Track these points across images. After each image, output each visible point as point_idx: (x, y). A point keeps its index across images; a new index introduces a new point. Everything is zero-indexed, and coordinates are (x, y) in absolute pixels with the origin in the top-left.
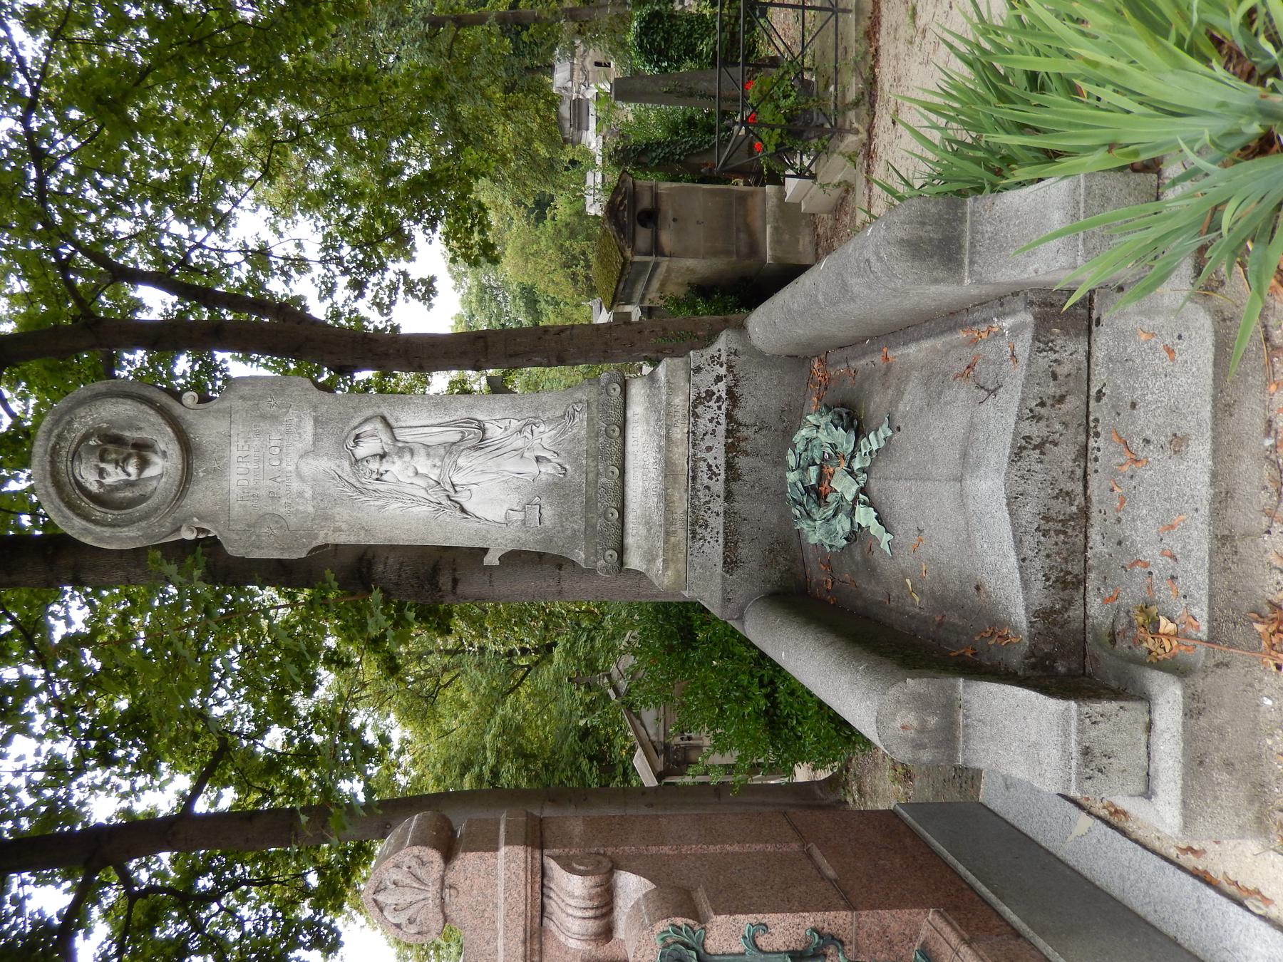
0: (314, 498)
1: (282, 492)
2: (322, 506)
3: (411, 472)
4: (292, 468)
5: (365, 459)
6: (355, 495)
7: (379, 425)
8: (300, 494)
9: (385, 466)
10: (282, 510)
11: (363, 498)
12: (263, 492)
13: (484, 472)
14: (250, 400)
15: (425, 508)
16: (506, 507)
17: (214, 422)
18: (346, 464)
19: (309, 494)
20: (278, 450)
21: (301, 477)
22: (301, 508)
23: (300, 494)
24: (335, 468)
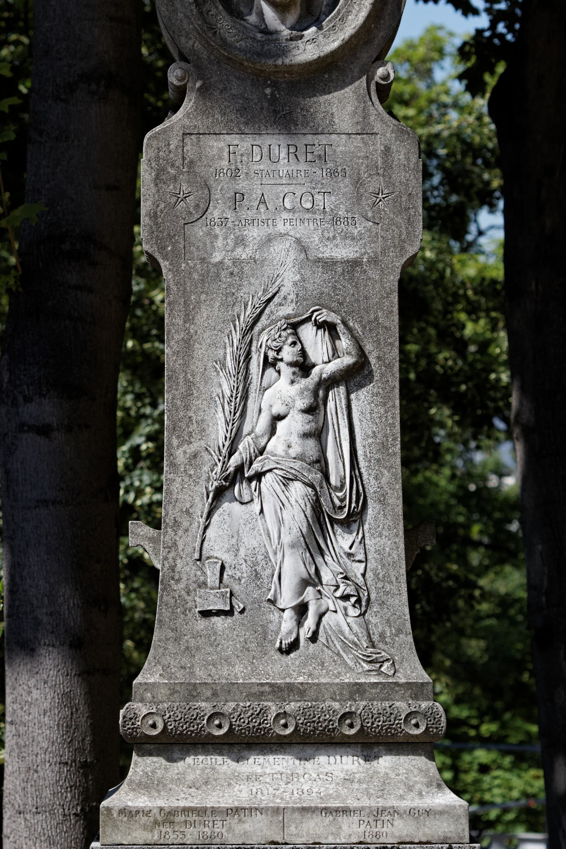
0: (236, 262)
1: (245, 214)
2: (223, 274)
3: (278, 409)
4: (281, 228)
5: (297, 341)
6: (241, 324)
7: (348, 360)
8: (241, 241)
9: (286, 371)
10: (216, 214)
11: (236, 337)
12: (242, 185)
13: (280, 522)
14: (385, 162)
15: (222, 433)
16: (228, 558)
17: (350, 108)
18: (288, 310)
19: (243, 254)
20: (308, 205)
21: (269, 240)
22: (220, 243)
23: (241, 241)
24: (282, 294)
